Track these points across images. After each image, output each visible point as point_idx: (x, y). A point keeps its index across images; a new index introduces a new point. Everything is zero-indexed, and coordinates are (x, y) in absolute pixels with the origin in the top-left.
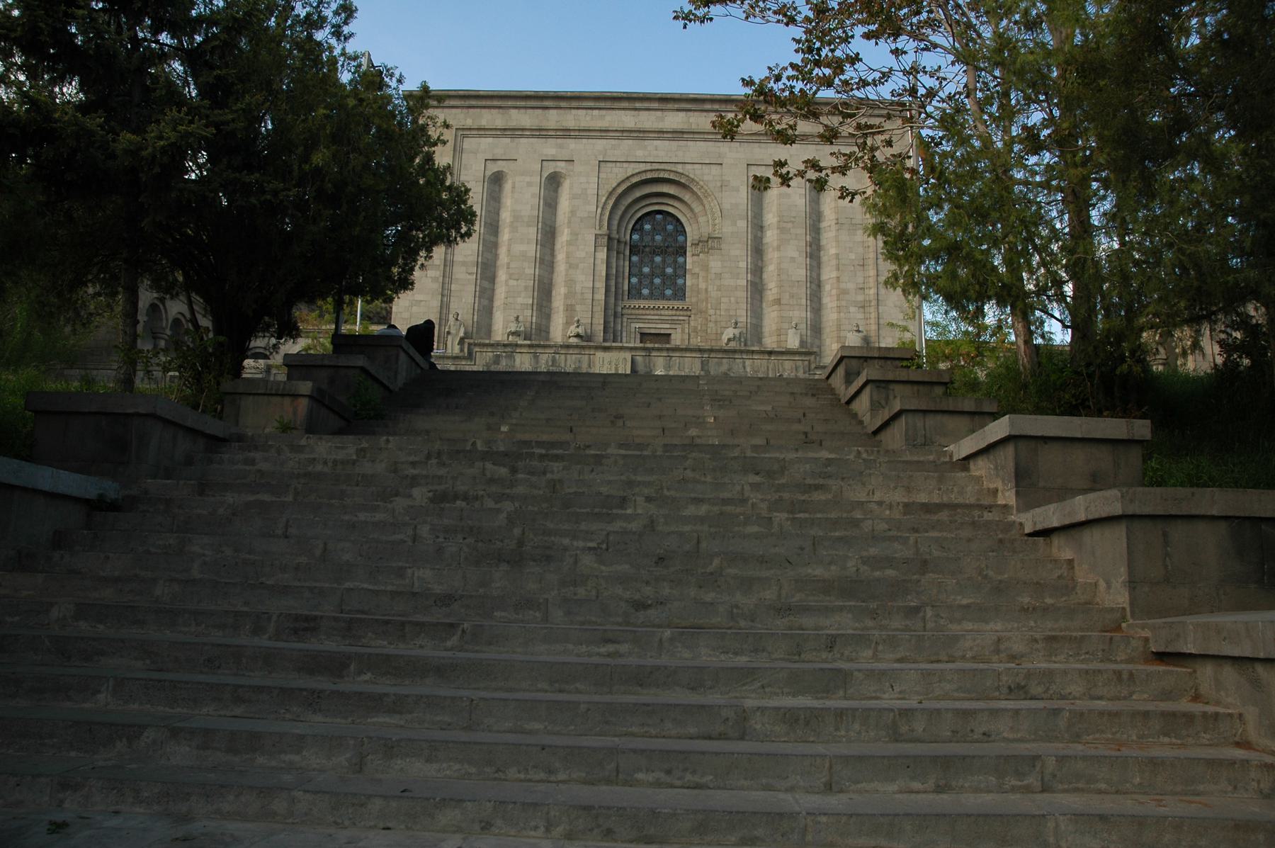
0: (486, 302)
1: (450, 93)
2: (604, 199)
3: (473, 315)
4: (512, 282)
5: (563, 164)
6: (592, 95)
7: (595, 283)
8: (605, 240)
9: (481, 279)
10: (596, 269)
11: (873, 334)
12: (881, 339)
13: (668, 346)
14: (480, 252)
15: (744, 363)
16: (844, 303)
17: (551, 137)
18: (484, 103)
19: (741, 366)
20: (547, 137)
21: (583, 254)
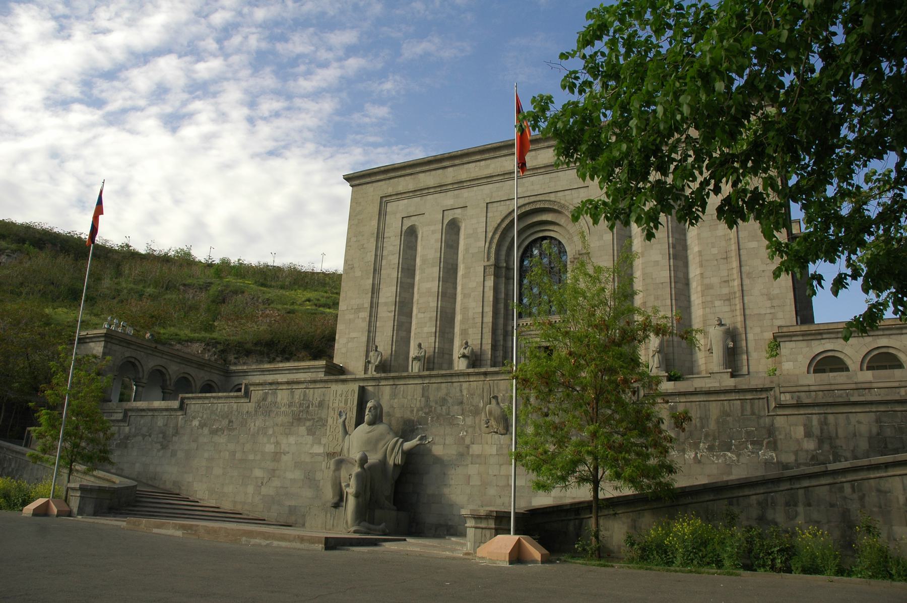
0: (403, 334)
1: (375, 170)
2: (490, 235)
3: (392, 345)
4: (422, 315)
5: (459, 211)
6: (477, 149)
7: (484, 308)
8: (492, 270)
9: (398, 315)
10: (485, 295)
11: (739, 326)
12: (748, 329)
13: (405, 374)
14: (398, 293)
15: (461, 386)
16: (709, 298)
17: (449, 190)
18: (399, 173)
19: (458, 389)
20: (446, 191)
21: (474, 284)
